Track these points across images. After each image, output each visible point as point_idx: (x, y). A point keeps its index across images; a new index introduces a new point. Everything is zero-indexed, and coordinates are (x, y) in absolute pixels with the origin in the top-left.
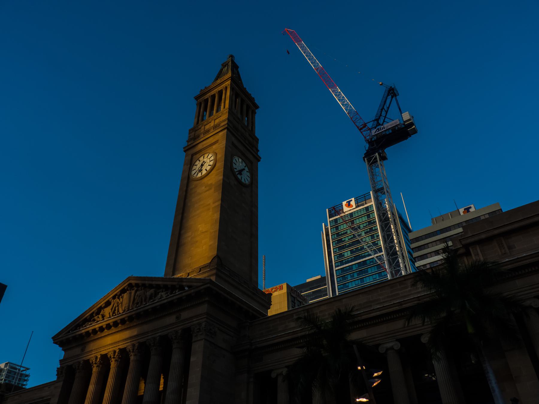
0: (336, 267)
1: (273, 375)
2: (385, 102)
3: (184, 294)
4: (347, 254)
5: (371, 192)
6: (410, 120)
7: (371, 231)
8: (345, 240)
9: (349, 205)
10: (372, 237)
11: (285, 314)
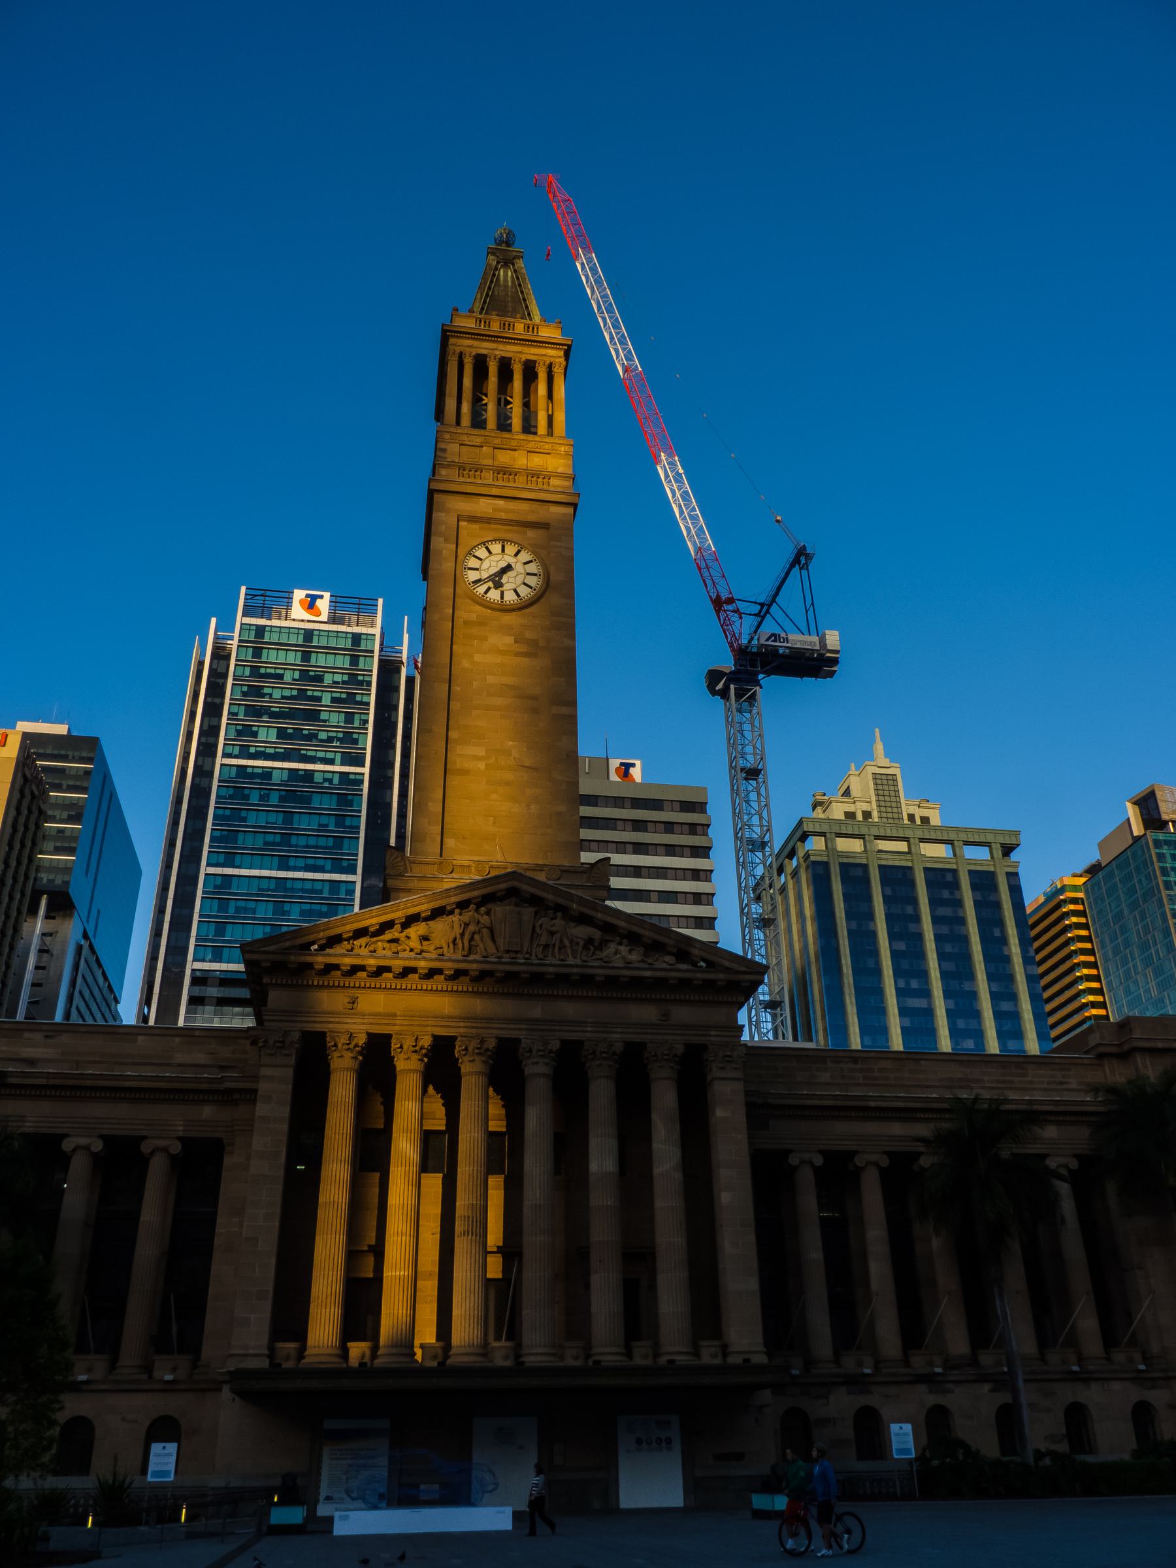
0: (225, 755)
1: (794, 1160)
2: (526, 404)
3: (699, 975)
4: (267, 734)
5: (381, 601)
6: (837, 652)
7: (349, 702)
8: (270, 695)
9: (311, 604)
10: (349, 717)
11: (811, 1053)
